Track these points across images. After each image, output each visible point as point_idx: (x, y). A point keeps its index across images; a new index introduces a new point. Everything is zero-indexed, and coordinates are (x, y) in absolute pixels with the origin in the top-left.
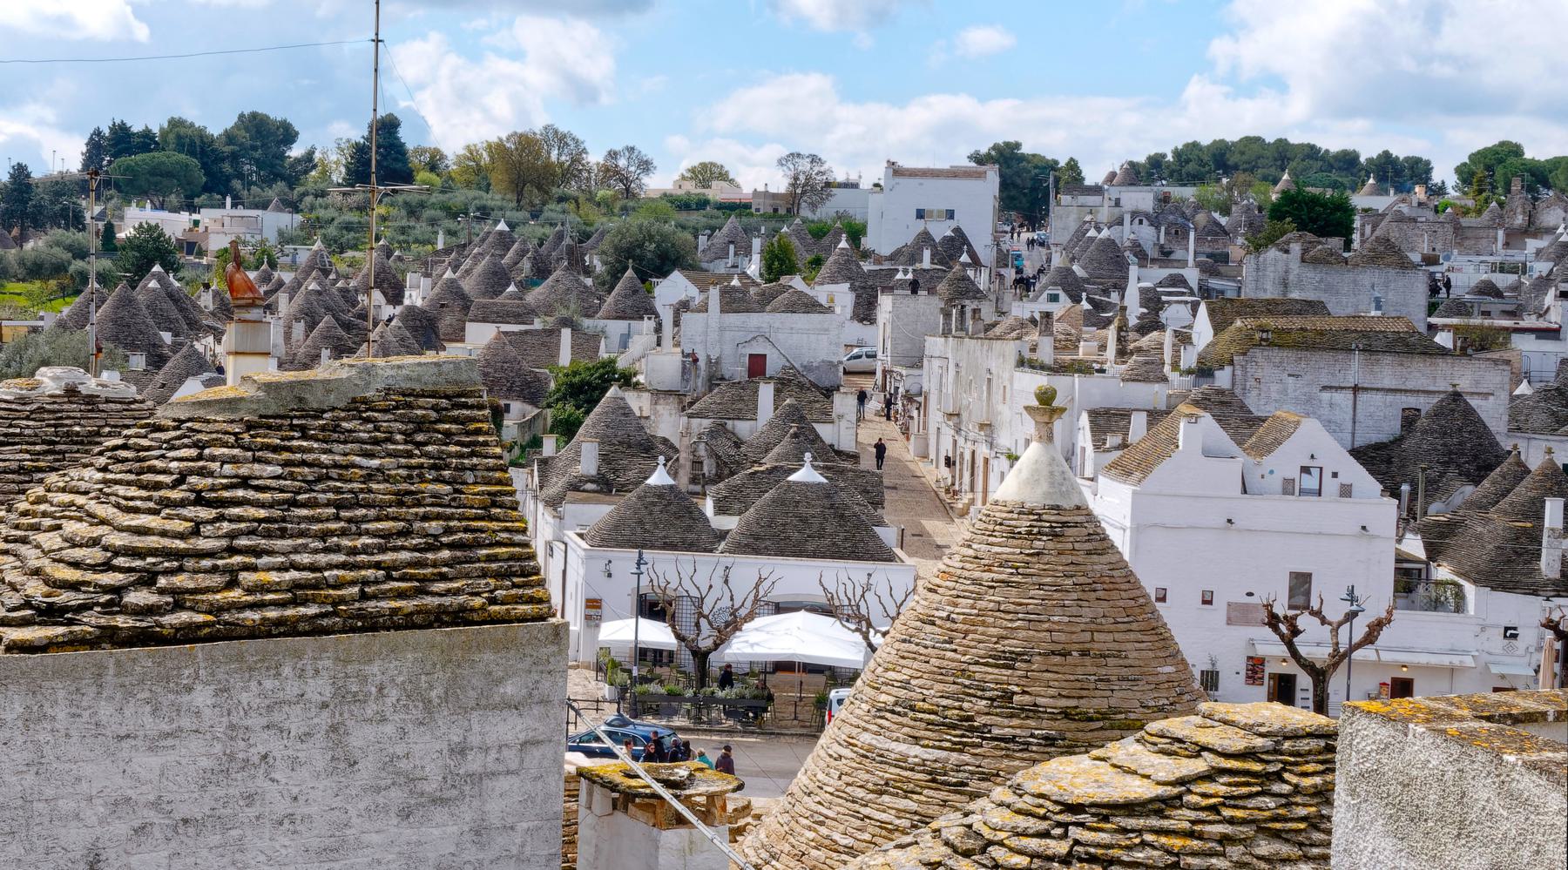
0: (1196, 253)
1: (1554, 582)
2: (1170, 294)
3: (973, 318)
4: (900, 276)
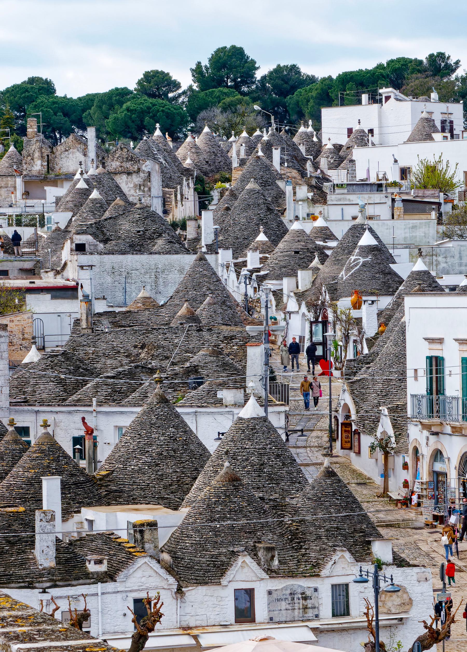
1: (50, 571)
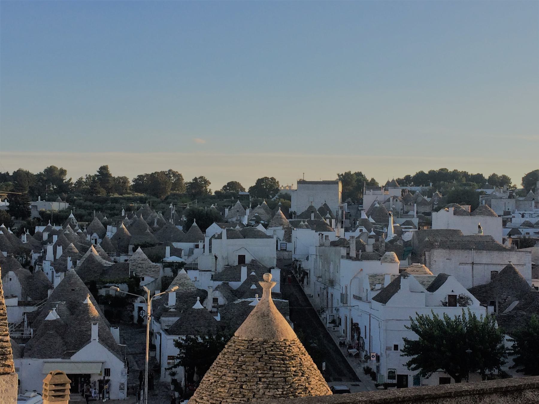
0: (417, 213)
2: (406, 228)
3: (326, 239)
4: (302, 223)
